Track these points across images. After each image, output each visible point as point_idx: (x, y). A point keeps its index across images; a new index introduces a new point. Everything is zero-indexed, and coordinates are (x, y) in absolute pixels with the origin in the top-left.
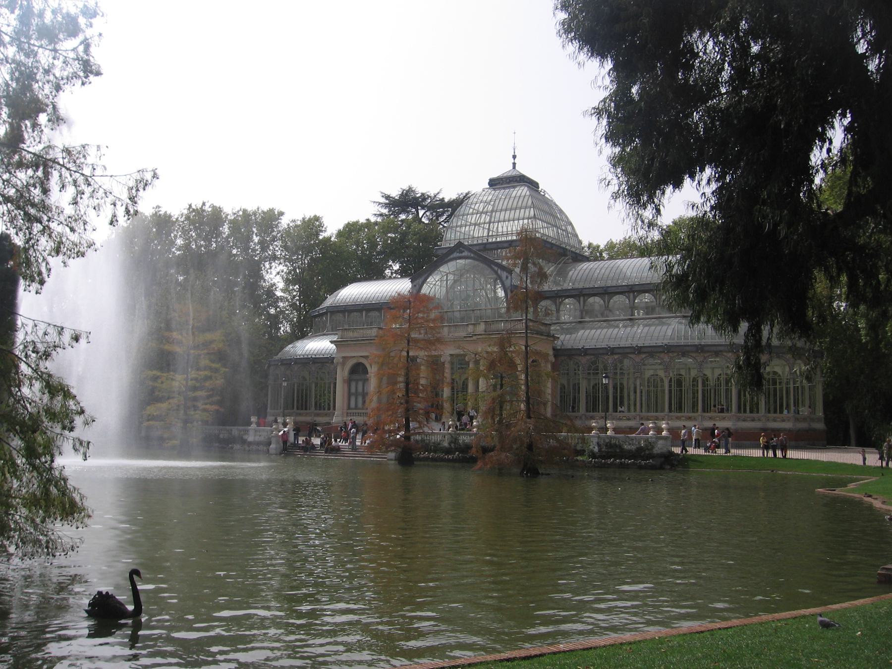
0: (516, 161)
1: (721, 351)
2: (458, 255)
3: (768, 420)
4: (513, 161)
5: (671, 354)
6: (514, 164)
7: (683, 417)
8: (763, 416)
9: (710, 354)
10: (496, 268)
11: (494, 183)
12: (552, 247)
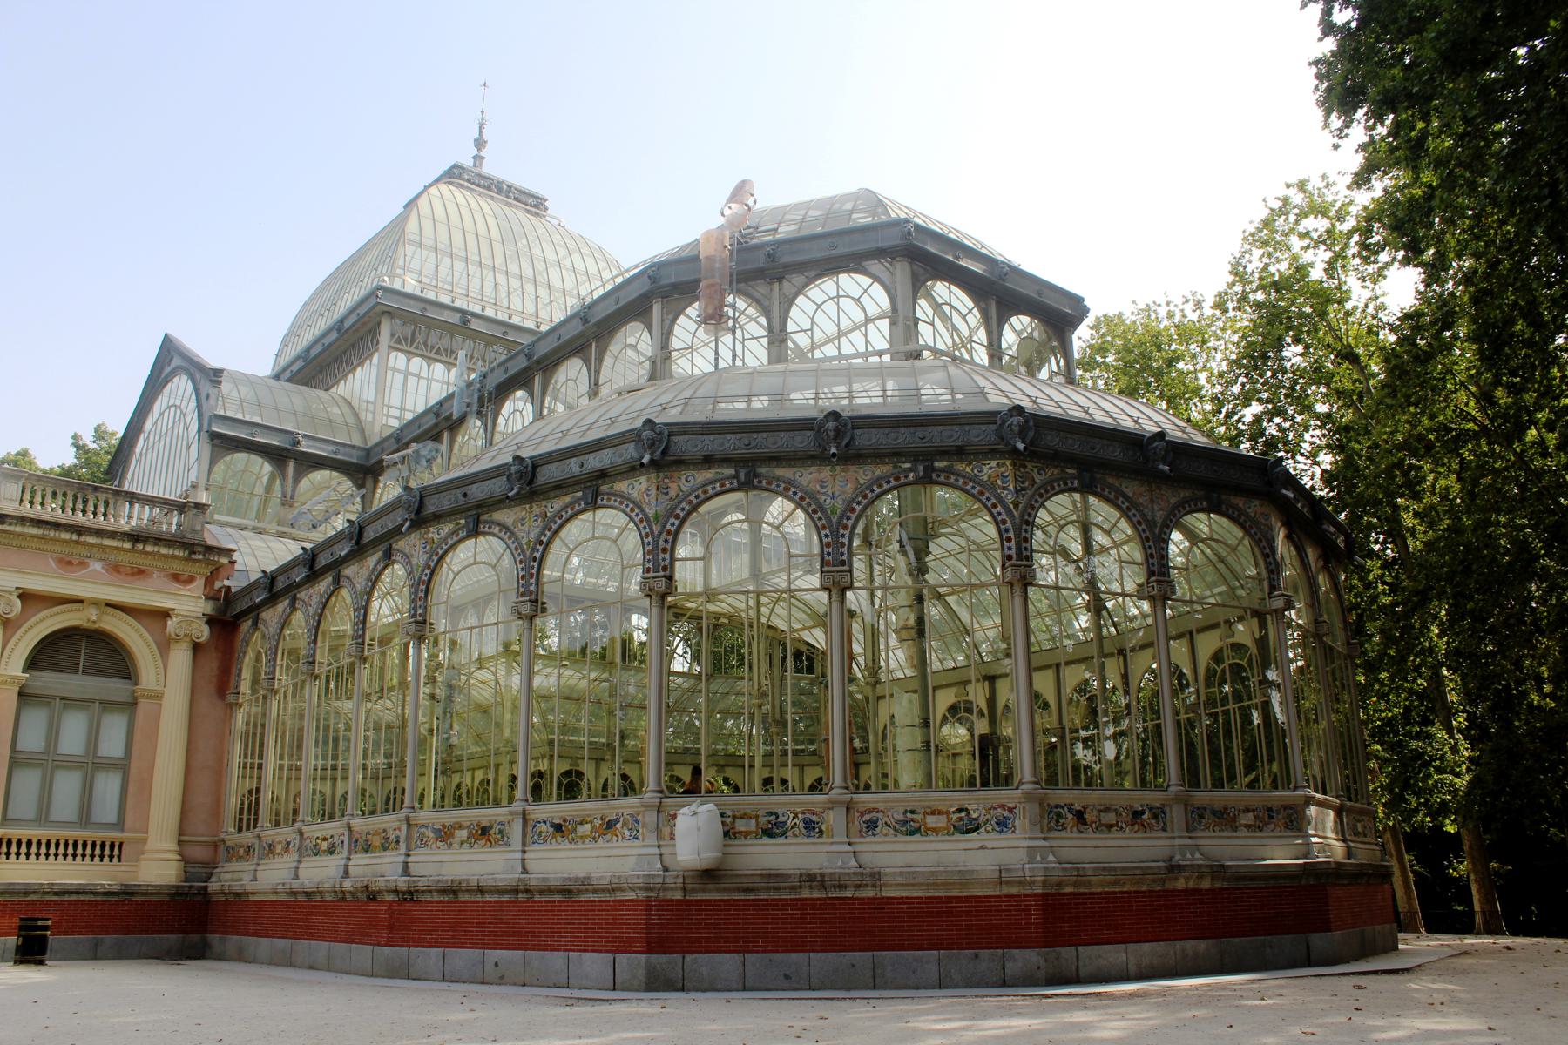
0: (482, 154)
1: (603, 475)
2: (168, 370)
3: (872, 825)
4: (475, 152)
5: (434, 533)
6: (478, 159)
7: (461, 827)
8: (833, 804)
9: (567, 499)
10: (198, 377)
11: (405, 207)
12: (466, 322)
